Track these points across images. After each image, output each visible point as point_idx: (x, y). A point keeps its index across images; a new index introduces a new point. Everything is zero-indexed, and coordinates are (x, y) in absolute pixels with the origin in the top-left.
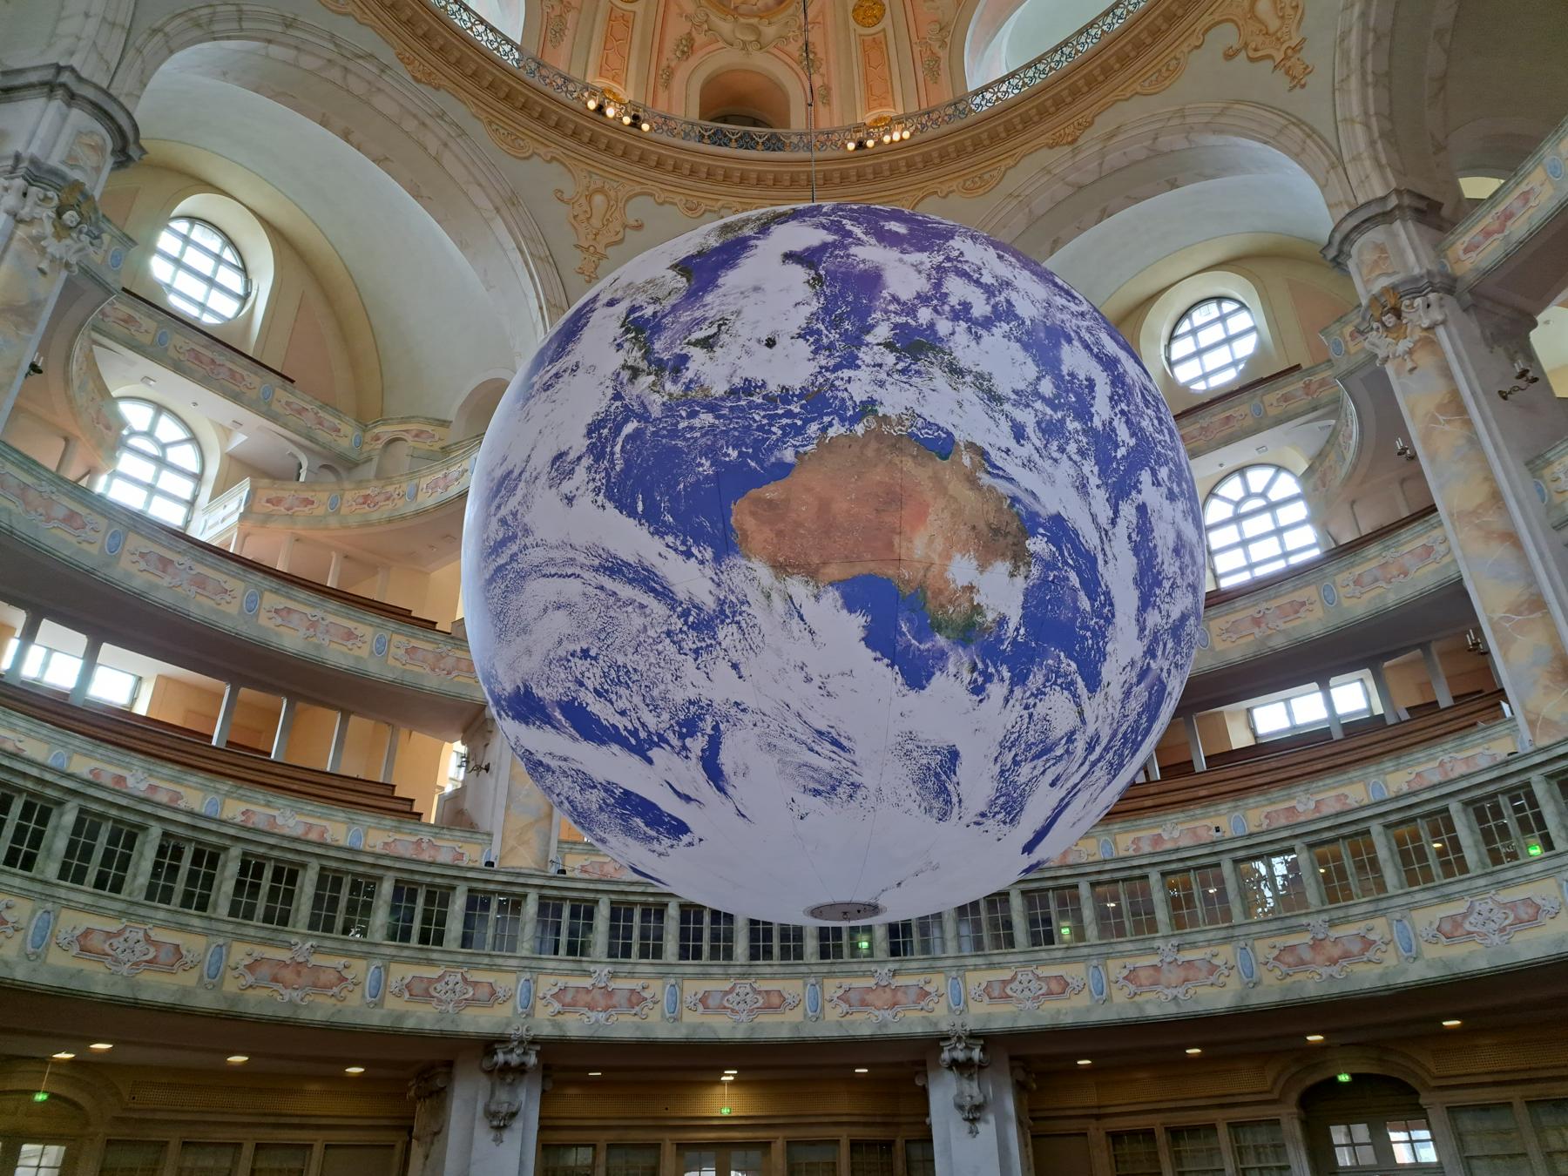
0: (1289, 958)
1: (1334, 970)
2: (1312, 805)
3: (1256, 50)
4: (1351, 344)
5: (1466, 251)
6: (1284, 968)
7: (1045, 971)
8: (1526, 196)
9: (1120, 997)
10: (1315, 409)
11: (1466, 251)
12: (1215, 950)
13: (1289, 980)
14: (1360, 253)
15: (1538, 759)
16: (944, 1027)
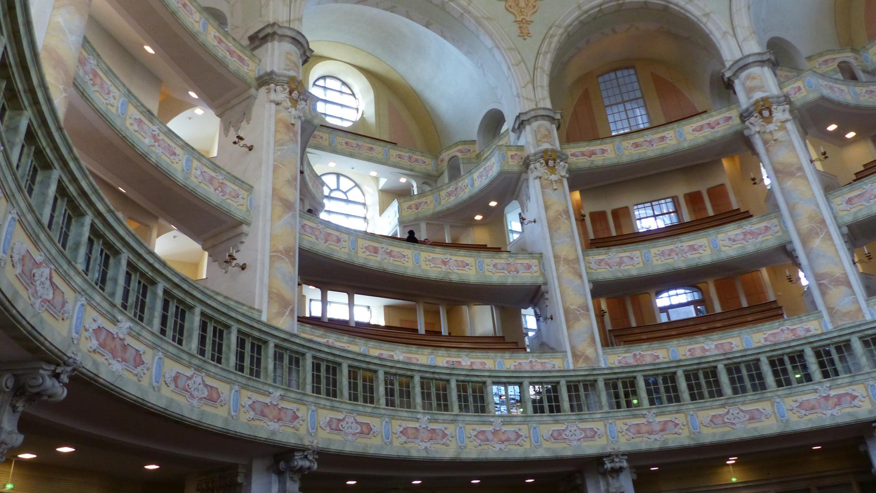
0: (481, 437)
1: (503, 446)
2: (469, 363)
3: (510, 6)
4: (510, 159)
5: (572, 155)
6: (479, 441)
7: (361, 419)
8: (603, 151)
9: (397, 443)
10: (411, 170)
11: (572, 155)
12: (446, 425)
13: (480, 448)
14: (539, 127)
15: (606, 372)
16: (306, 442)
